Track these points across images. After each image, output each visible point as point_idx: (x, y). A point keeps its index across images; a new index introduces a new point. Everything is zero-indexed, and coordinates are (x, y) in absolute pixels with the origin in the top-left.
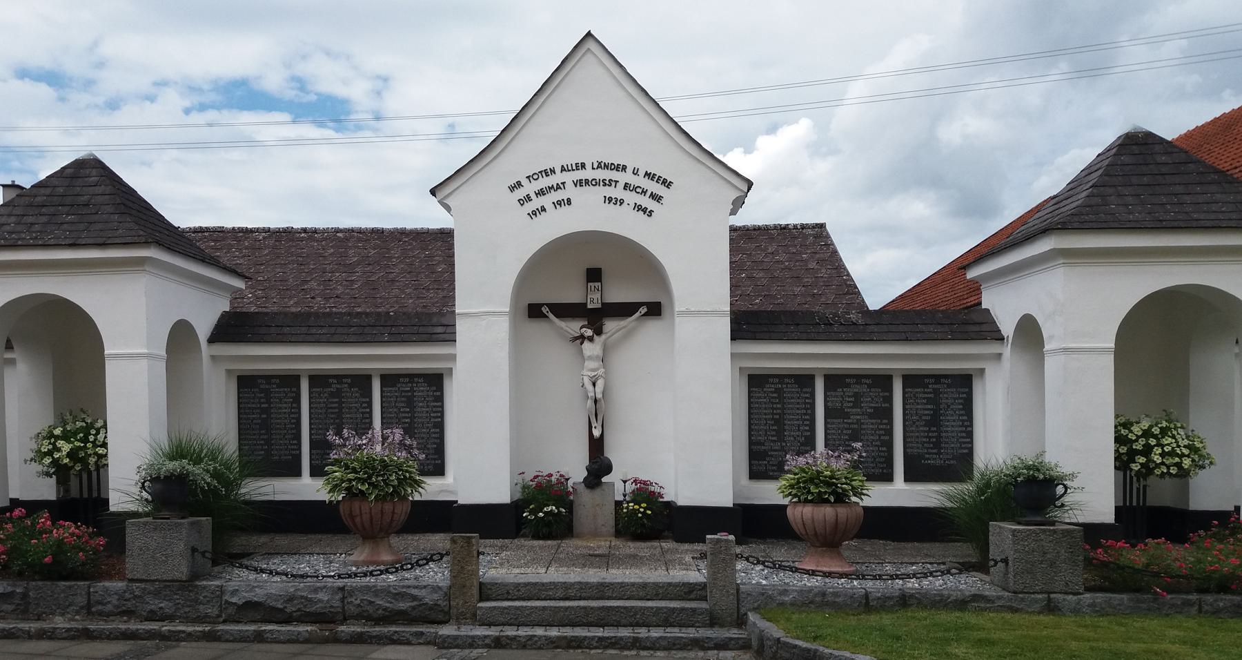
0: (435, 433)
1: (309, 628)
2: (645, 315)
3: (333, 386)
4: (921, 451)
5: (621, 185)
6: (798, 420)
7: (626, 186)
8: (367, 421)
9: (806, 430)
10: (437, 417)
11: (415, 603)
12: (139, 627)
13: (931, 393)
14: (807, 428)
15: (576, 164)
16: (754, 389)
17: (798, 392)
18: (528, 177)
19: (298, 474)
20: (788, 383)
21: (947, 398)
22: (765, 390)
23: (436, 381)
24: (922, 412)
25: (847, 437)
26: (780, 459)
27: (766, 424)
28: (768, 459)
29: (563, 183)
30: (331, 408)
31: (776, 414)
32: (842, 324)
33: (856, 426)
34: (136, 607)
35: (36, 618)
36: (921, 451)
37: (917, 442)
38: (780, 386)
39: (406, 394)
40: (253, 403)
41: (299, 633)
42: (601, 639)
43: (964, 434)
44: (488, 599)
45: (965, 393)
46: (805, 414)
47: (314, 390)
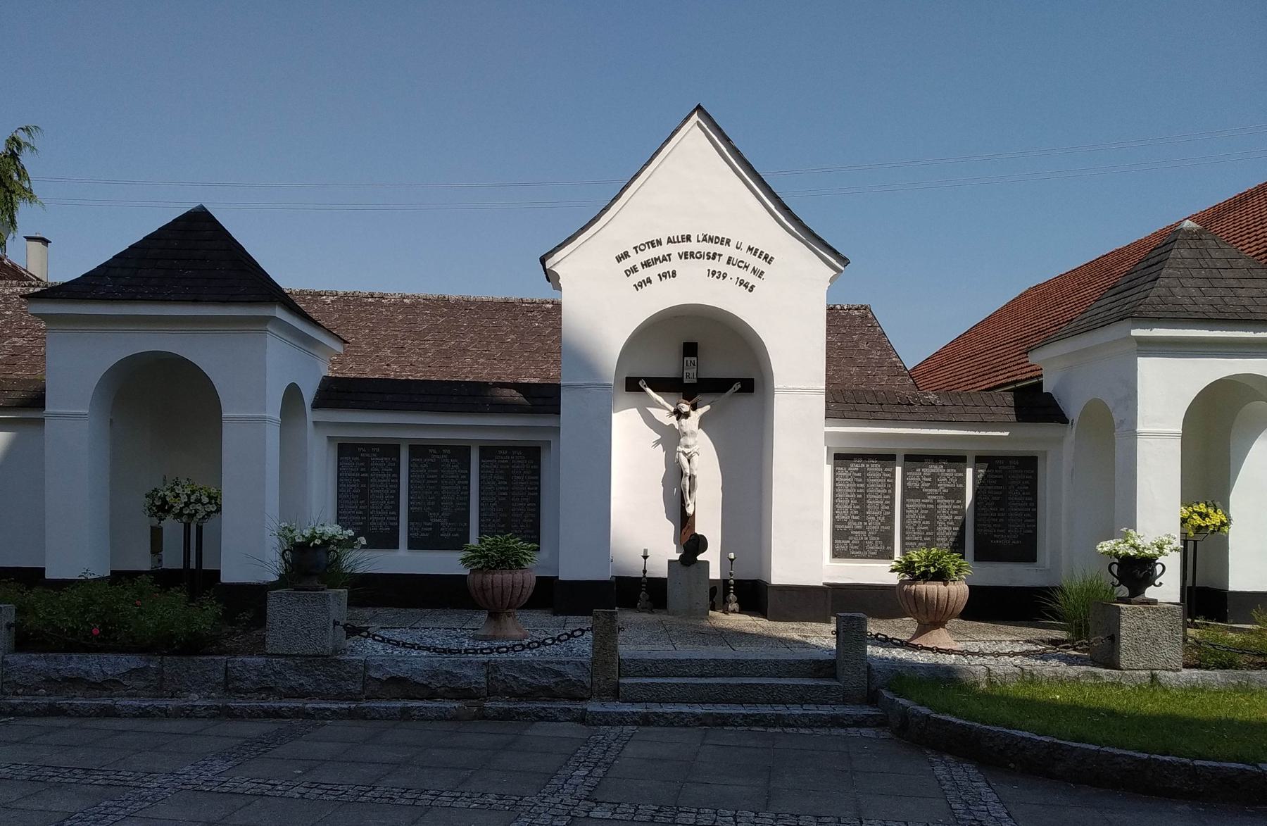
1: (456, 705)
2: (739, 391)
4: (990, 531)
5: (724, 259)
6: (879, 499)
7: (729, 260)
8: (466, 493)
9: (887, 510)
10: (534, 491)
11: (559, 679)
12: (282, 705)
13: (1000, 474)
14: (888, 508)
15: (682, 236)
17: (880, 472)
18: (635, 248)
19: (396, 547)
22: (849, 469)
23: (532, 454)
24: (991, 493)
25: (924, 517)
26: (862, 538)
27: (849, 504)
28: (850, 538)
29: (669, 255)
30: (430, 479)
31: (859, 493)
32: (922, 405)
33: (932, 506)
34: (276, 683)
35: (170, 694)
36: (990, 531)
37: (987, 523)
38: (864, 466)
40: (353, 472)
41: (447, 710)
42: (745, 716)
43: (1029, 515)
44: (627, 676)
46: (886, 494)
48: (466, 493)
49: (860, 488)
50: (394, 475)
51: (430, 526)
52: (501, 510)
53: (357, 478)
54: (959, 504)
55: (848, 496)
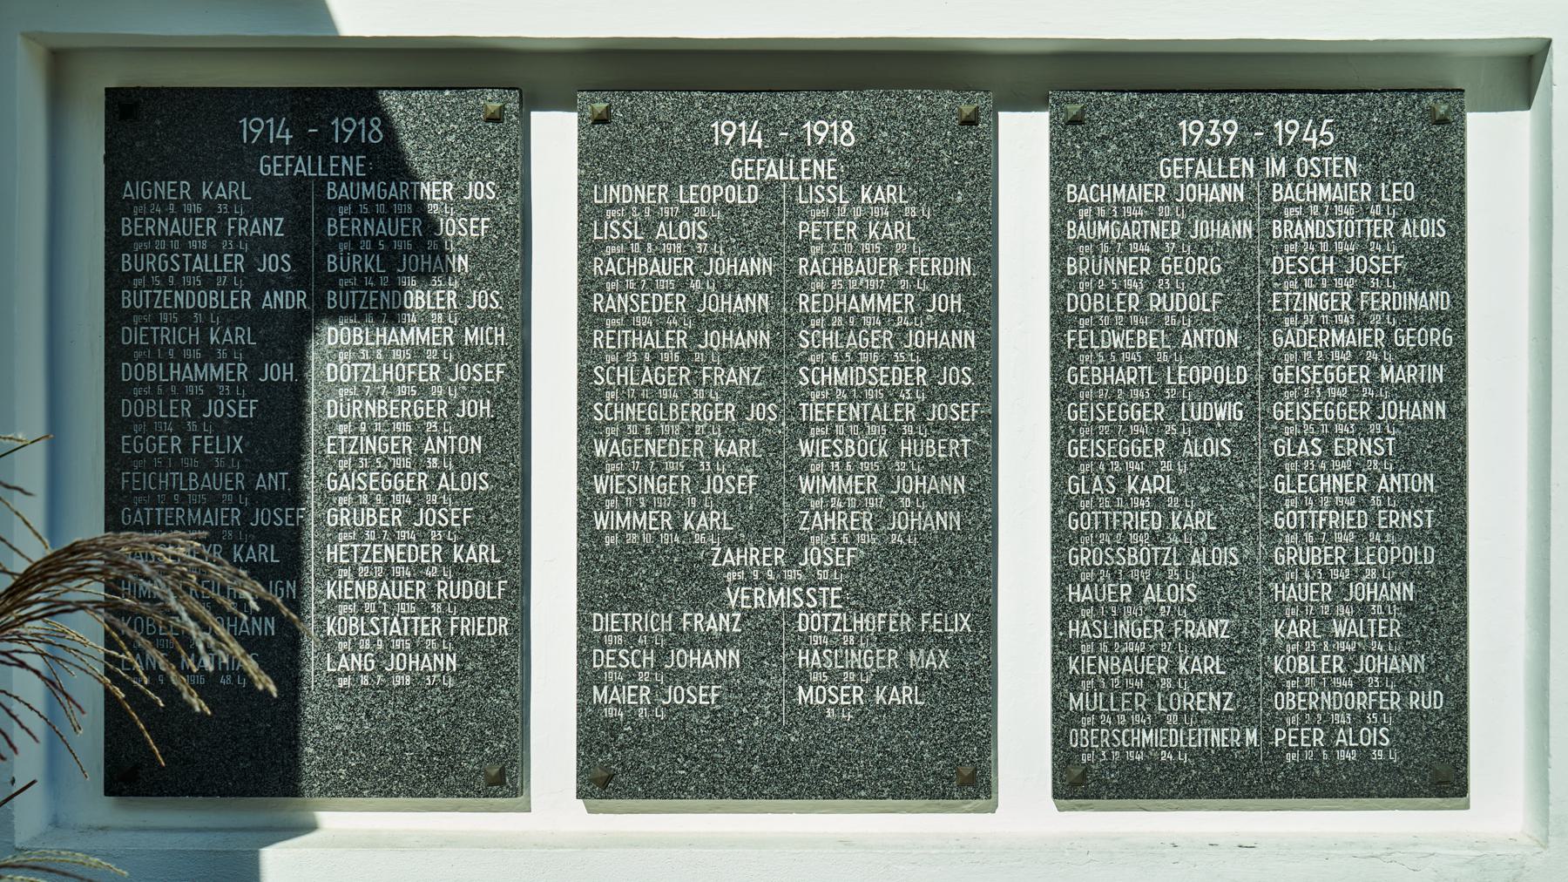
0: (1407, 501)
3: (741, 169)
8: (961, 412)
10: (1420, 391)
30: (727, 322)
39: (1224, 231)
40: (209, 281)
47: (614, 192)
48: (961, 412)
50: (481, 299)
51: (725, 641)
52: (1202, 520)
53: (231, 318)
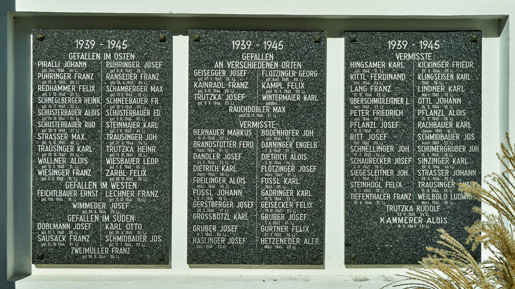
4: (378, 197)
6: (134, 131)
9: (151, 155)
14: (152, 149)
16: (44, 64)
20: (115, 50)
21: (431, 83)
22: (66, 65)
25: (232, 169)
31: (89, 119)
33: (249, 144)
36: (378, 197)
37: (371, 179)
43: (463, 161)
45: (465, 71)
46: (149, 119)
49: (91, 107)
54: (310, 139)
55: (64, 124)
